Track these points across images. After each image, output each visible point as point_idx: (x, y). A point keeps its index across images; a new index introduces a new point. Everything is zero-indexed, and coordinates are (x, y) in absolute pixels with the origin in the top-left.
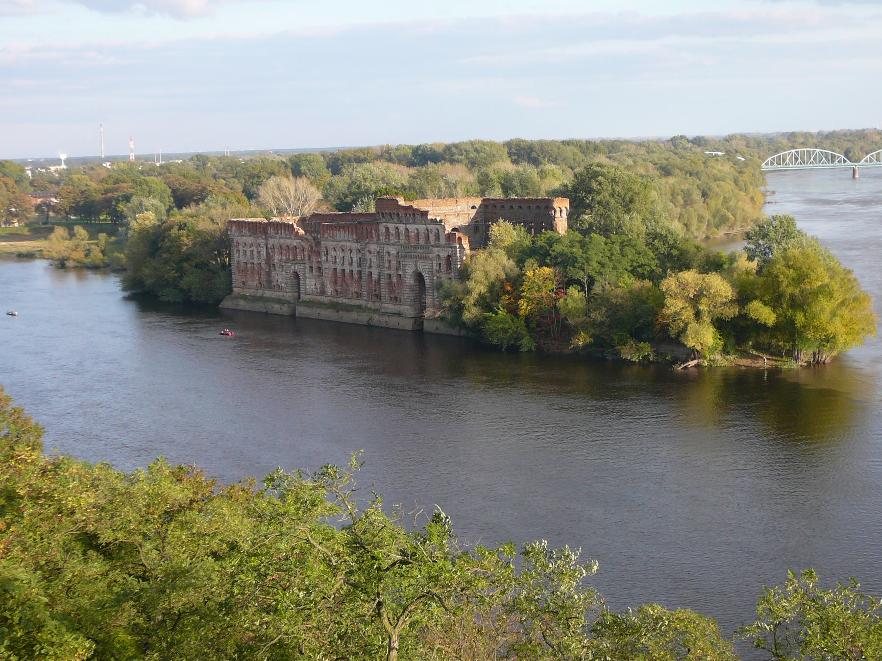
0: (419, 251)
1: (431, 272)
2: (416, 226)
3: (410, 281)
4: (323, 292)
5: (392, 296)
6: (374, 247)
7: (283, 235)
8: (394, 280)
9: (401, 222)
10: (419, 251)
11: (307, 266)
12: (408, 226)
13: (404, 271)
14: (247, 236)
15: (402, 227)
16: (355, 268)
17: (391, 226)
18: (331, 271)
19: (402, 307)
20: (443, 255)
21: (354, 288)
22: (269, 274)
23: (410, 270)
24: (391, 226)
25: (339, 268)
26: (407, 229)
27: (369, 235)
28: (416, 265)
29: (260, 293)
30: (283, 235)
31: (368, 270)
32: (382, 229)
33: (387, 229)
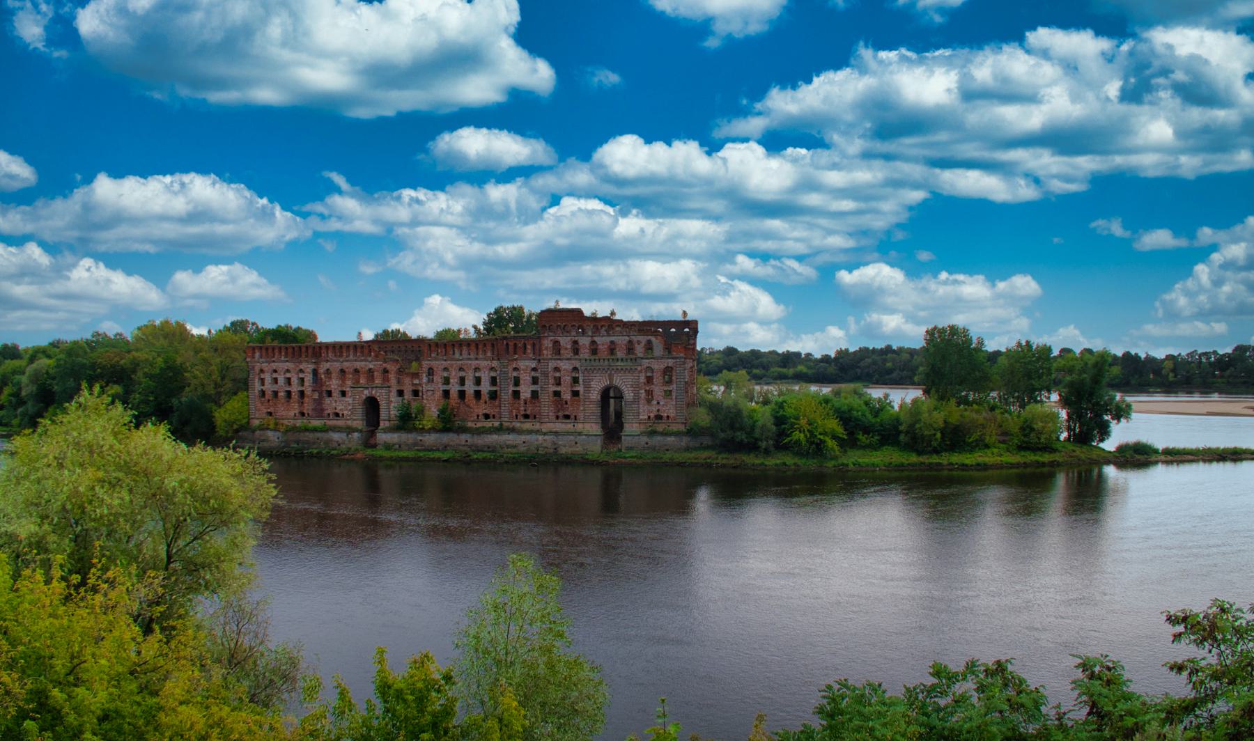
1: (636, 387)
3: (595, 396)
5: (560, 414)
6: (526, 364)
8: (567, 396)
9: (584, 333)
12: (596, 339)
13: (587, 386)
15: (584, 341)
16: (485, 387)
17: (565, 341)
18: (439, 394)
19: (580, 426)
20: (658, 366)
21: (482, 409)
22: (319, 402)
23: (598, 384)
24: (565, 341)
25: (454, 388)
26: (593, 342)
29: (299, 423)
30: (351, 357)
31: (512, 388)
32: (547, 343)
33: (556, 343)
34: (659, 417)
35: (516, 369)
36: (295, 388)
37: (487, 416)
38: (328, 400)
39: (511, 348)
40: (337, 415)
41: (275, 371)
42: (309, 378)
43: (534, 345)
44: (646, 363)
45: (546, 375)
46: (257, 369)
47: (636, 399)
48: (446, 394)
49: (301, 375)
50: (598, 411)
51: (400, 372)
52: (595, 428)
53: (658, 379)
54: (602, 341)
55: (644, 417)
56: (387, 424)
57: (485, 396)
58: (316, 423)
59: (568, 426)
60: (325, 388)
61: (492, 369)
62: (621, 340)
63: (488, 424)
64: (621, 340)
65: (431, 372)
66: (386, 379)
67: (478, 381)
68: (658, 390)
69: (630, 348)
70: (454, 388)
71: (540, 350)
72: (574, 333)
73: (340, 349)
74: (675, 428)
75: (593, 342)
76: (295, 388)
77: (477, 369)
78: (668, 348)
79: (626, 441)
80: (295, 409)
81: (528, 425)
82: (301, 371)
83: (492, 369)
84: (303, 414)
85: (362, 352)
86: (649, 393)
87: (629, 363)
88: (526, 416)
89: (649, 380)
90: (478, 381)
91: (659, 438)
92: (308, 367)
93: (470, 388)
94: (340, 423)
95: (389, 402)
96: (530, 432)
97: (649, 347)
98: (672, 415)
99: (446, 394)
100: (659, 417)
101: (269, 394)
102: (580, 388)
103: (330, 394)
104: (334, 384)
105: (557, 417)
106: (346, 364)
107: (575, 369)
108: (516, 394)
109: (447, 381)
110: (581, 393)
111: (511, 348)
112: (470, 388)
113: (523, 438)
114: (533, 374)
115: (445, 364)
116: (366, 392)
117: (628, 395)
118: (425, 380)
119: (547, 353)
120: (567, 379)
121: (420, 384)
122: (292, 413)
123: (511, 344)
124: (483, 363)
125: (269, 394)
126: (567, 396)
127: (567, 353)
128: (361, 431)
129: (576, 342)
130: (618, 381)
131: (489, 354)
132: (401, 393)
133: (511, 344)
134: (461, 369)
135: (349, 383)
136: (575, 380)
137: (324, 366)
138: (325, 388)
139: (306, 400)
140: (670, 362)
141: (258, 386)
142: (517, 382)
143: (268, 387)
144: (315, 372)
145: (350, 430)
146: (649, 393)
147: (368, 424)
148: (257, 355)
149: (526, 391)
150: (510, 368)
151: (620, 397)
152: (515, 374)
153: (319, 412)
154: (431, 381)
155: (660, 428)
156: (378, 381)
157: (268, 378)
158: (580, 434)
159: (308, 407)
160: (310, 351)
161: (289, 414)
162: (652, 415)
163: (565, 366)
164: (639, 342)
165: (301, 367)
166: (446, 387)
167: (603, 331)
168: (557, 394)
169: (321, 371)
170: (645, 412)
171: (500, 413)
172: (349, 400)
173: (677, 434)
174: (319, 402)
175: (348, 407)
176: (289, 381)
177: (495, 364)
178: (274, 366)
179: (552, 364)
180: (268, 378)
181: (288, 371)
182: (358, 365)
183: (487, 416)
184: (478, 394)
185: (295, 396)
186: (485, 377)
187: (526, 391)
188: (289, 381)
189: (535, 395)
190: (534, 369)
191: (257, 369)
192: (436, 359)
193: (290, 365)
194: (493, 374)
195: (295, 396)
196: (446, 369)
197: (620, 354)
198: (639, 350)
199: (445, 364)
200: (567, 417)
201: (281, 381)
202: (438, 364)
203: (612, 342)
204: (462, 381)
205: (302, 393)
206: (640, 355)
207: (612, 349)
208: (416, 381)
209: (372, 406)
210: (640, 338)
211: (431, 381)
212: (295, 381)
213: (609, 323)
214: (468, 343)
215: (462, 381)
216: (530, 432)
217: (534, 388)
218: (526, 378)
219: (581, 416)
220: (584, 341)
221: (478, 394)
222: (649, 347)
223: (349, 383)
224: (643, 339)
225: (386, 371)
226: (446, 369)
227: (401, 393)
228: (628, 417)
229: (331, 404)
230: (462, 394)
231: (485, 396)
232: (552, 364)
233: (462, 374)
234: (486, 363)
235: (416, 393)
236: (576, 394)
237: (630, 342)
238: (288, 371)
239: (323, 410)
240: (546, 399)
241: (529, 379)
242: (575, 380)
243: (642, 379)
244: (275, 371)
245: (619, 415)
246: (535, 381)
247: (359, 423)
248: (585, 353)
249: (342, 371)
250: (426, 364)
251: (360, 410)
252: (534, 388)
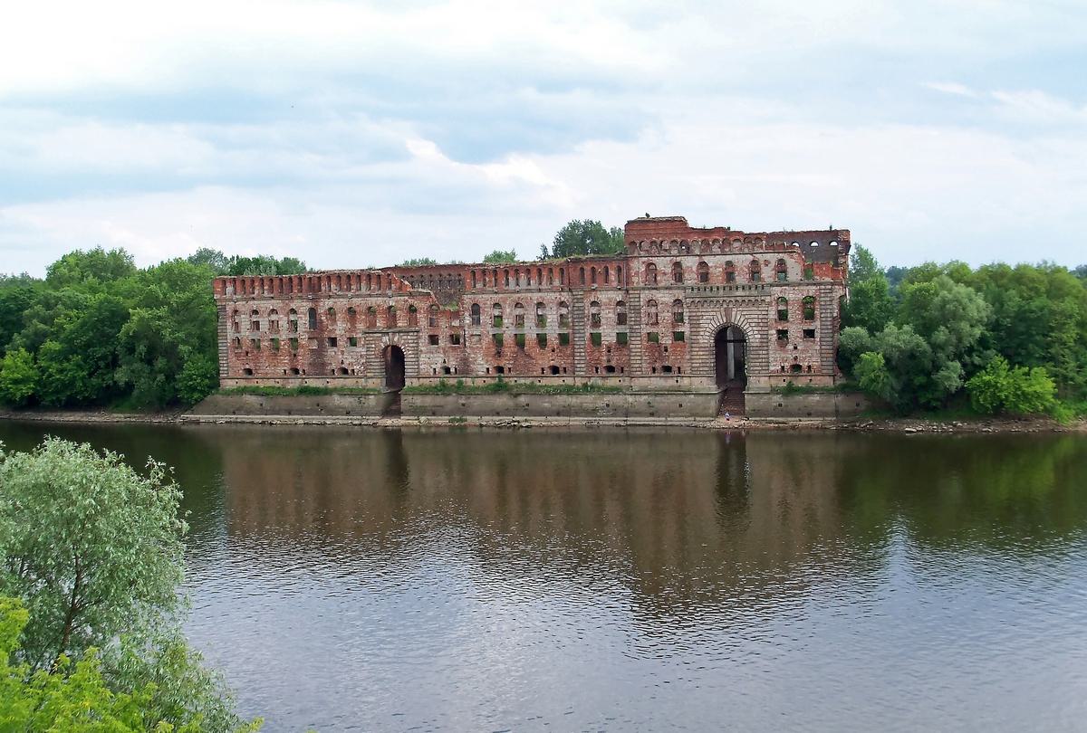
0: (740, 292)
1: (763, 324)
2: (729, 258)
3: (706, 339)
4: (465, 369)
5: (657, 365)
6: (608, 296)
7: (364, 290)
8: (667, 341)
9: (689, 252)
10: (739, 293)
11: (424, 336)
12: (706, 259)
13: (695, 325)
14: (265, 299)
15: (690, 263)
16: (552, 331)
17: (663, 264)
18: (487, 340)
19: (686, 381)
20: (794, 295)
21: (546, 359)
22: (319, 353)
23: (710, 321)
25: (508, 332)
26: (703, 264)
27: (600, 278)
28: (728, 314)
29: (294, 383)
30: (364, 290)
31: (589, 330)
32: (638, 266)
34: (796, 368)
35: (594, 304)
36: (284, 335)
37: (555, 370)
38: (331, 351)
39: (588, 273)
40: (345, 371)
41: (255, 312)
42: (303, 321)
43: (619, 270)
44: (777, 291)
45: (637, 310)
46: (229, 309)
47: (765, 341)
48: (498, 341)
49: (292, 317)
50: (711, 361)
51: (432, 311)
52: (707, 384)
53: (794, 313)
54: (716, 262)
55: (775, 367)
56: (416, 383)
57: (553, 340)
58: (313, 383)
59: (671, 383)
60: (326, 335)
61: (562, 304)
62: (742, 261)
63: (556, 381)
64: (742, 261)
65: (476, 309)
66: (413, 321)
67: (541, 320)
68: (795, 329)
69: (755, 271)
70: (508, 332)
71: (629, 276)
72: (674, 252)
73: (346, 279)
74: (819, 381)
75: (703, 264)
76: (284, 335)
77: (540, 305)
78: (807, 272)
79: (750, 402)
80: (284, 363)
81: (613, 382)
82: (293, 311)
83: (562, 304)
84: (296, 371)
85: (379, 283)
86: (783, 334)
87: (754, 292)
88: (610, 369)
89: (783, 316)
90: (541, 320)
91: (800, 398)
92: (303, 306)
93: (531, 331)
94: (349, 382)
95: (417, 353)
96: (615, 391)
97: (781, 268)
98: (815, 362)
99: (498, 341)
100: (796, 368)
101: (246, 345)
102: (685, 329)
103: (333, 342)
104: (340, 328)
105: (654, 370)
106: (356, 301)
107: (678, 302)
108: (596, 340)
109: (498, 320)
110: (687, 334)
111: (588, 273)
112: (531, 331)
113: (608, 399)
114: (619, 309)
115: (497, 298)
116: (386, 339)
117: (753, 337)
118: (468, 320)
119: (637, 281)
120: (666, 316)
121: (461, 327)
122: (280, 370)
123: (587, 269)
124: (551, 297)
125: (246, 345)
126: (667, 341)
127: (664, 281)
128: (377, 393)
129: (677, 265)
130: (738, 317)
131: (557, 283)
132: (433, 340)
133: (587, 269)
134: (518, 305)
135: (361, 326)
136: (679, 318)
137: (325, 304)
138: (326, 335)
139: (301, 351)
140: (812, 290)
141: (230, 333)
142: (596, 322)
143: (246, 333)
144: (313, 312)
145: (361, 393)
146: (783, 334)
147: (389, 384)
148: (230, 289)
149: (609, 334)
150: (587, 302)
151: (741, 339)
152: (594, 310)
153: (320, 368)
154: (476, 322)
155: (801, 382)
156: (401, 323)
157: (245, 321)
158: (687, 392)
159: (303, 361)
160: (305, 283)
161: (273, 373)
162: (787, 365)
163: (665, 297)
164: (767, 263)
165: (293, 306)
166: (496, 331)
167: (716, 249)
168: (652, 338)
169: (321, 311)
170: (778, 359)
171: (574, 365)
172: (360, 350)
173: (823, 391)
174: (319, 353)
175: (358, 359)
176: (274, 325)
177: (565, 297)
178: (254, 305)
179: (645, 295)
180: (245, 321)
181: (273, 311)
182: (373, 301)
183: (555, 370)
184: (542, 340)
185: (284, 345)
186: (552, 316)
187: (609, 334)
188: (274, 325)
189: (622, 340)
190: (620, 303)
191: (229, 309)
192: (483, 292)
193: (276, 304)
194: (564, 311)
195: (284, 345)
196: (497, 305)
197: (741, 279)
198: (767, 274)
199: (497, 298)
200: (668, 369)
201: (264, 325)
202: (486, 300)
203: (729, 264)
204: (520, 321)
205: (294, 341)
206: (770, 280)
207: (729, 273)
208: (456, 323)
209: (395, 361)
210: (768, 257)
211: (476, 322)
212: (284, 323)
213: (724, 237)
214: (528, 269)
215: (520, 321)
216: (615, 391)
217: (622, 329)
218: (608, 315)
219: (686, 367)
220: (690, 263)
221: (542, 340)
222: (781, 268)
223: (361, 326)
224: (773, 258)
225: (412, 310)
226: (497, 305)
227: (433, 340)
228: (752, 366)
229: (334, 357)
230: (520, 342)
231: (553, 340)
232: (645, 295)
233: (519, 311)
234: (552, 296)
235: (455, 340)
236: (679, 337)
237: (754, 262)
238: (273, 311)
239: (323, 365)
240: (637, 345)
241: (613, 317)
242: (679, 318)
243: (773, 314)
244: (255, 312)
245: (740, 366)
246: (622, 319)
247: (377, 382)
248: (691, 279)
249: (351, 312)
250: (468, 299)
251: (377, 364)
252: (622, 329)
